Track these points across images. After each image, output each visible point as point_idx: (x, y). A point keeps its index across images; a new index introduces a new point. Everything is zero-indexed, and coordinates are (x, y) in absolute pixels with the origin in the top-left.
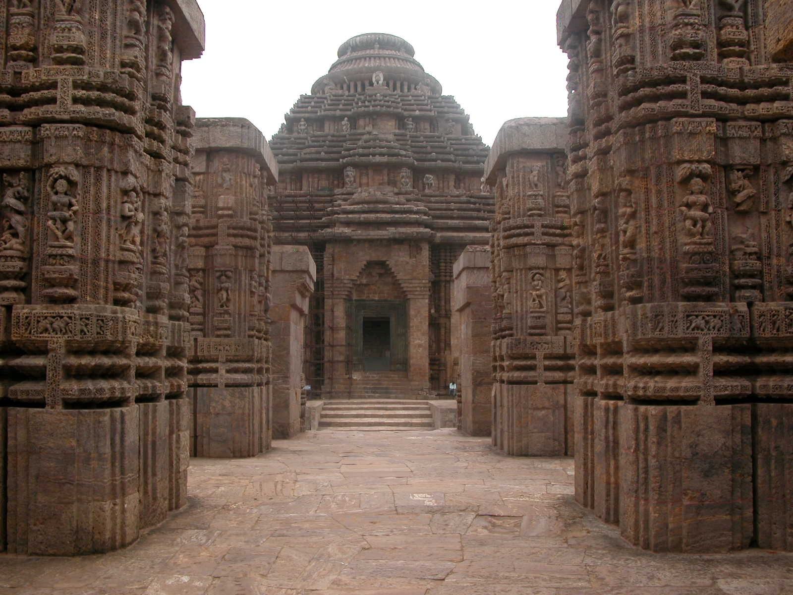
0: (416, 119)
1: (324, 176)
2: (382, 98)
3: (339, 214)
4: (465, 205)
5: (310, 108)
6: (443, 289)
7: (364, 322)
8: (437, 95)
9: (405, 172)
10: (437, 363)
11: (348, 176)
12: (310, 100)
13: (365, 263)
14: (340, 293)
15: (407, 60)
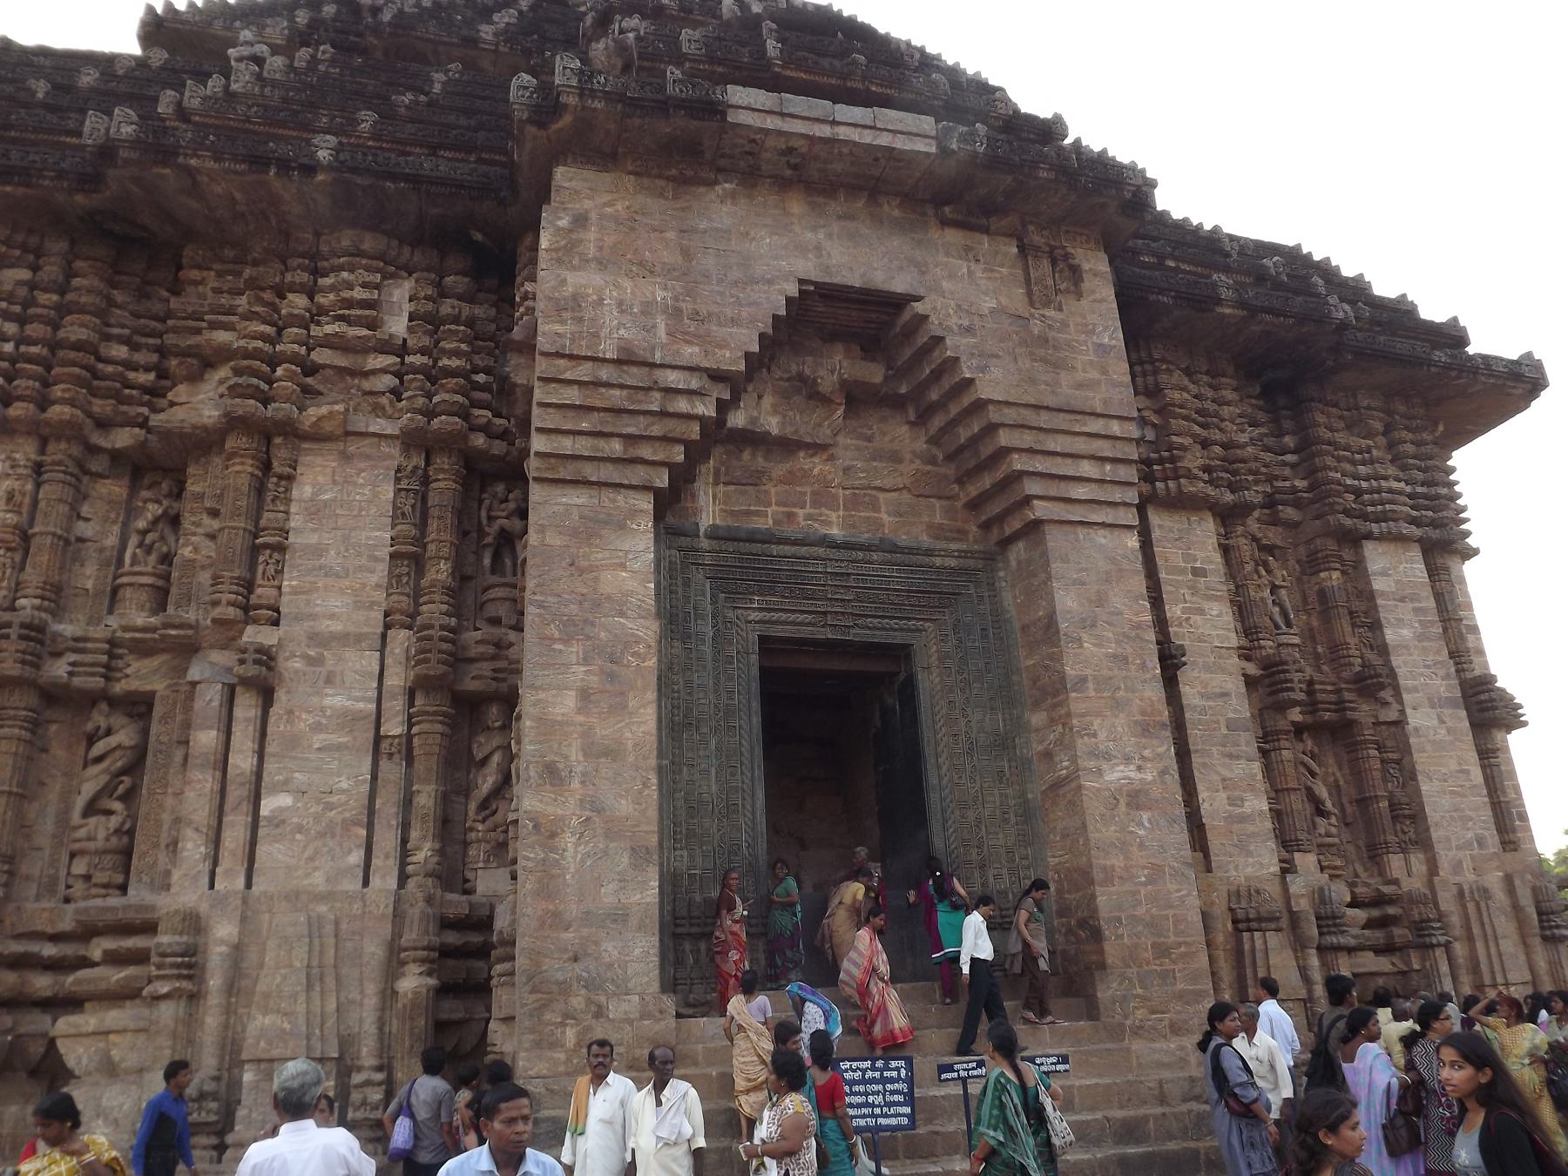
7: (762, 669)
13: (793, 290)
14: (646, 452)
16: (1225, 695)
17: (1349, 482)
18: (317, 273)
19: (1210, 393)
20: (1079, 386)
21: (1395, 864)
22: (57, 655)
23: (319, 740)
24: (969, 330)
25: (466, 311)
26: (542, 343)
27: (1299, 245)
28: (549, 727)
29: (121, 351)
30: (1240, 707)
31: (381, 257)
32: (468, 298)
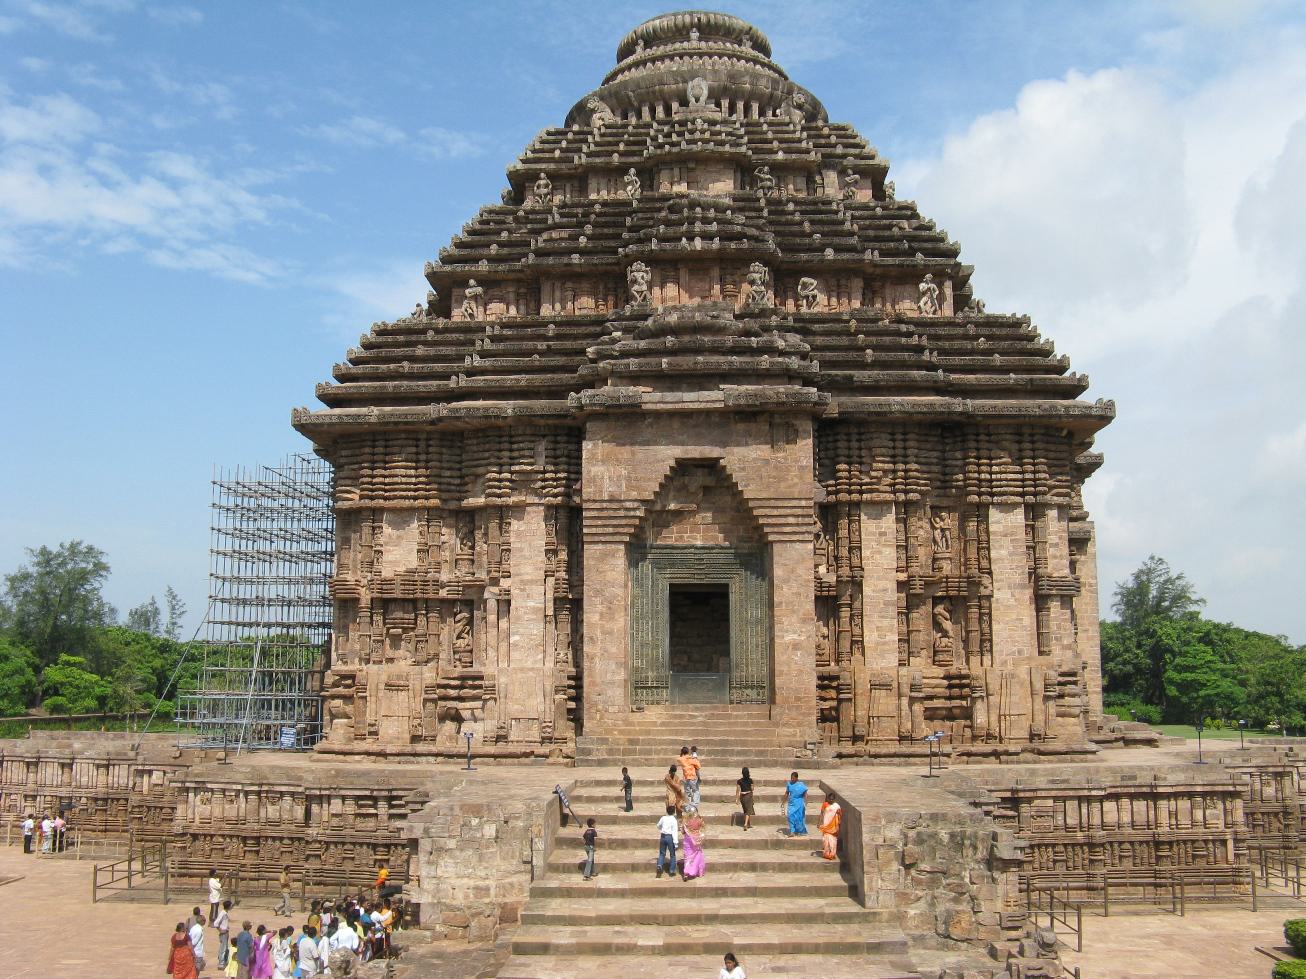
0: (779, 170)
1: (585, 285)
2: (706, 126)
3: (616, 358)
4: (887, 339)
5: (557, 153)
6: (844, 522)
7: (672, 594)
8: (820, 123)
9: (758, 272)
10: (835, 684)
11: (635, 281)
12: (560, 137)
13: (672, 463)
14: (621, 530)
15: (756, 61)
16: (885, 590)
17: (983, 476)
18: (512, 443)
19: (899, 444)
20: (790, 487)
21: (975, 660)
22: (442, 588)
23: (526, 617)
24: (744, 469)
25: (566, 452)
26: (585, 497)
27: (1014, 315)
28: (591, 625)
29: (448, 473)
30: (893, 595)
31: (533, 435)
32: (567, 442)
